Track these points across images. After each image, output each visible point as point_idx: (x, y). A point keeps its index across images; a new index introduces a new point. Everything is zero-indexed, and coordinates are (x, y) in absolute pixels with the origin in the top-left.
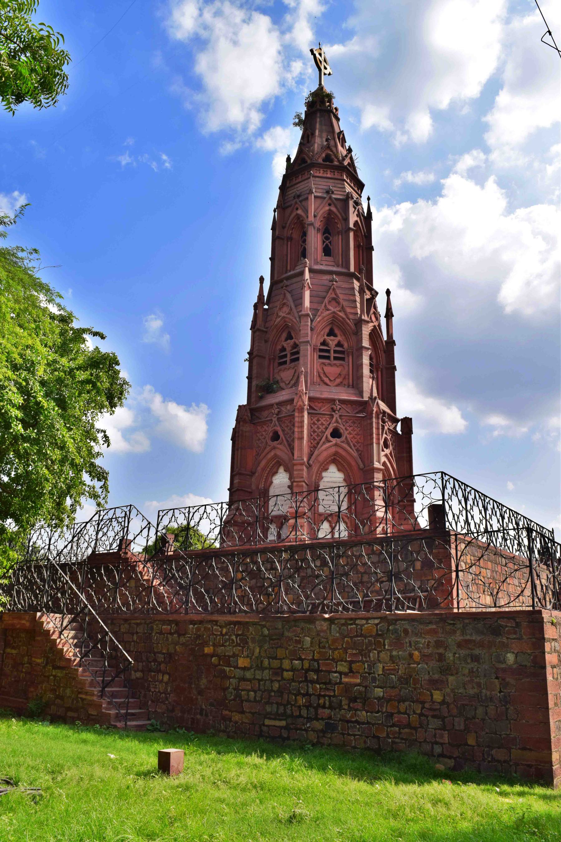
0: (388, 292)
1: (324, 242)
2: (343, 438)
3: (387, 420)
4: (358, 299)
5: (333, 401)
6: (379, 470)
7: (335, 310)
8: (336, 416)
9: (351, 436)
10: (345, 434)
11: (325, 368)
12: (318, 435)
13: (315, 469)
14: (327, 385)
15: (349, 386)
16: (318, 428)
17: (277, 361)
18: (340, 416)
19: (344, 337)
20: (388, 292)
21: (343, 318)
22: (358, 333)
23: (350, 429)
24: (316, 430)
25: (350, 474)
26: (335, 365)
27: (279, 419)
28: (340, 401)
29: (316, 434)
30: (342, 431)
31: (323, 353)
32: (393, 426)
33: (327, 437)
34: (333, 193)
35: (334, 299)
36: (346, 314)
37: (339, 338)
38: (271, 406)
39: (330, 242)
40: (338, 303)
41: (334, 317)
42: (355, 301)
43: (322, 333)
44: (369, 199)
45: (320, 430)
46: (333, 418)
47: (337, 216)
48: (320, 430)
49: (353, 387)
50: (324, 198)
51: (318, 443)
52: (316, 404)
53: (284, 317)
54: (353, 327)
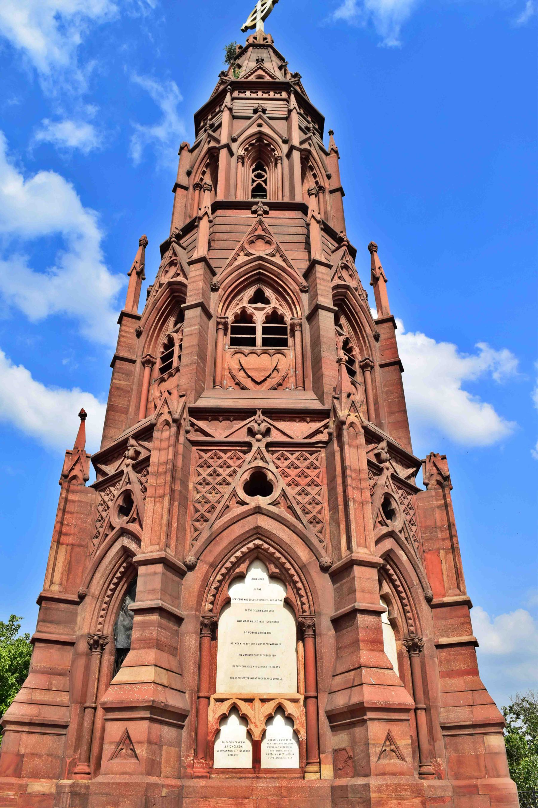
0: (372, 249)
1: (253, 181)
7: (263, 255)
8: (258, 445)
10: (280, 485)
14: (243, 388)
17: (159, 364)
18: (268, 445)
23: (293, 473)
26: (265, 352)
27: (134, 467)
34: (264, 111)
35: (260, 237)
37: (273, 305)
38: (127, 440)
39: (265, 181)
44: (331, 133)
50: (249, 118)
53: (170, 284)
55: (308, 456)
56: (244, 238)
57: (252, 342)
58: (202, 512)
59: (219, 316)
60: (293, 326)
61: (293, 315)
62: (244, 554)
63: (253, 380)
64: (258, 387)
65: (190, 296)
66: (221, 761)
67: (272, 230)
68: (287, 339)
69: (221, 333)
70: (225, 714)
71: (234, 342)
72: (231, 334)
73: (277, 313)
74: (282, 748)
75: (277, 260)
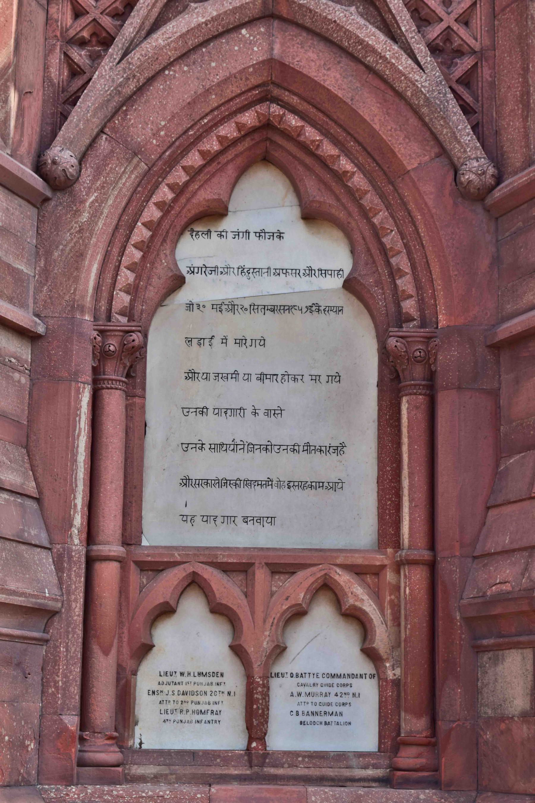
13: (100, 203)
58: (94, 14)
62: (228, 145)
70: (167, 603)
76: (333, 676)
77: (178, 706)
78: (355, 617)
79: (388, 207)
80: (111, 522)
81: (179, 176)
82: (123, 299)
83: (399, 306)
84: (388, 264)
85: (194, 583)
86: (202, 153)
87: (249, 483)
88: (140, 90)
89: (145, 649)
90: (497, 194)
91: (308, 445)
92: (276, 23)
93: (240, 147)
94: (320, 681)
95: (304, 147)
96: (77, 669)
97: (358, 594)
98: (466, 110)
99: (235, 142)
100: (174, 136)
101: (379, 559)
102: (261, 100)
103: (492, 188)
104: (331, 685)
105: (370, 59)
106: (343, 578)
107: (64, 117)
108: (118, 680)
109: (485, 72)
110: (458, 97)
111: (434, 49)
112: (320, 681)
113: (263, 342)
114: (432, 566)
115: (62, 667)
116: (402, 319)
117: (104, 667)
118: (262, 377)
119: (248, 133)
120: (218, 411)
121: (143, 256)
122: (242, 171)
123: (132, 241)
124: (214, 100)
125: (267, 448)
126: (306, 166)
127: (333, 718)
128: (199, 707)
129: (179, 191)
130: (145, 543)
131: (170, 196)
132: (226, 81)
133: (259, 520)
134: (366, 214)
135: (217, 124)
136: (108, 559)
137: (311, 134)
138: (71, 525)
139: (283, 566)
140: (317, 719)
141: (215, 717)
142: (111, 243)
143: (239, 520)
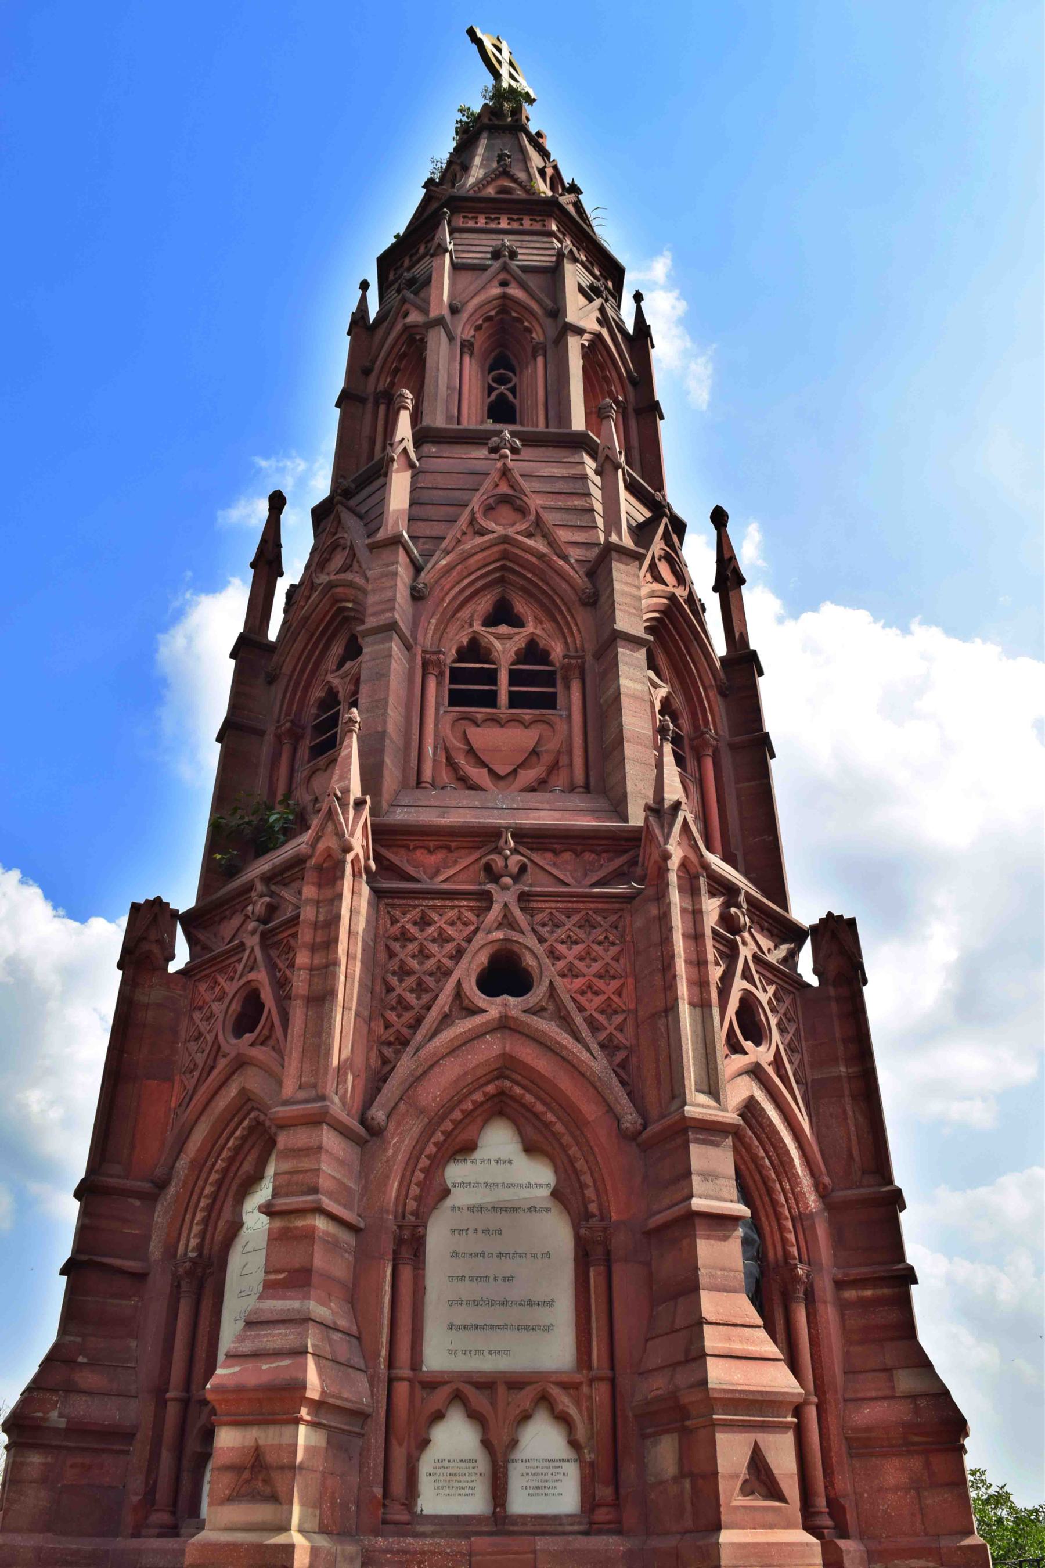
0: (719, 518)
2: (538, 994)
3: (745, 920)
4: (598, 507)
5: (487, 837)
6: (712, 1131)
7: (510, 532)
8: (504, 897)
9: (579, 982)
11: (473, 732)
12: (420, 988)
13: (400, 1143)
15: (572, 789)
16: (423, 954)
18: (523, 898)
19: (548, 625)
20: (719, 518)
21: (541, 556)
22: (597, 596)
24: (414, 964)
25: (581, 1164)
28: (521, 835)
29: (411, 981)
30: (529, 961)
31: (469, 684)
32: (783, 950)
33: (459, 993)
35: (505, 500)
36: (552, 543)
37: (531, 628)
40: (522, 511)
41: (505, 556)
42: (593, 510)
43: (465, 614)
45: (430, 964)
46: (489, 908)
47: (531, 312)
48: (430, 964)
49: (587, 788)
51: (419, 1021)
52: (420, 855)
54: (579, 579)
55: (599, 919)
56: (476, 502)
57: (490, 699)
58: (398, 1026)
59: (429, 649)
60: (566, 668)
61: (568, 650)
62: (477, 1105)
63: (491, 771)
64: (502, 783)
65: (375, 614)
66: (433, 1501)
67: (526, 485)
68: (555, 693)
69: (432, 683)
71: (456, 699)
72: (451, 682)
73: (537, 644)
74: (548, 1474)
75: (538, 544)
76: (550, 1461)
77: (447, 1484)
78: (563, 1419)
79: (577, 1143)
80: (404, 1354)
81: (448, 1125)
82: (412, 1205)
83: (586, 1208)
84: (579, 1179)
85: (458, 1397)
86: (462, 1111)
87: (492, 1327)
88: (425, 1073)
89: (425, 1443)
90: (644, 1135)
91: (530, 1301)
92: (507, 1031)
93: (486, 1106)
94: (541, 1464)
95: (524, 1106)
96: (382, 1456)
97: (565, 1402)
98: (623, 1083)
99: (482, 1103)
100: (445, 1101)
101: (578, 1378)
102: (497, 1078)
103: (640, 1133)
104: (548, 1468)
105: (564, 1053)
106: (555, 1391)
107: (379, 1090)
108: (408, 1464)
109: (634, 1060)
110: (618, 1075)
111: (602, 1046)
112: (541, 1464)
113: (499, 1232)
114: (613, 1381)
115: (372, 1454)
116: (588, 1216)
117: (399, 1454)
118: (500, 1255)
119: (490, 1098)
120: (472, 1279)
121: (425, 1178)
122: (486, 1121)
123: (418, 1167)
124: (469, 1078)
125: (503, 1303)
126: (527, 1119)
127: (551, 1491)
128: (461, 1485)
129: (448, 1134)
130: (424, 1369)
131: (442, 1138)
132: (478, 1066)
133: (499, 1352)
134: (564, 1149)
135: (470, 1093)
136: (402, 1379)
137: (529, 1098)
138: (379, 1356)
139: (516, 1382)
140: (539, 1491)
141: (471, 1491)
142: (405, 1169)
143: (486, 1353)
